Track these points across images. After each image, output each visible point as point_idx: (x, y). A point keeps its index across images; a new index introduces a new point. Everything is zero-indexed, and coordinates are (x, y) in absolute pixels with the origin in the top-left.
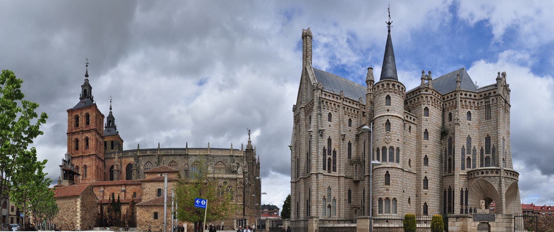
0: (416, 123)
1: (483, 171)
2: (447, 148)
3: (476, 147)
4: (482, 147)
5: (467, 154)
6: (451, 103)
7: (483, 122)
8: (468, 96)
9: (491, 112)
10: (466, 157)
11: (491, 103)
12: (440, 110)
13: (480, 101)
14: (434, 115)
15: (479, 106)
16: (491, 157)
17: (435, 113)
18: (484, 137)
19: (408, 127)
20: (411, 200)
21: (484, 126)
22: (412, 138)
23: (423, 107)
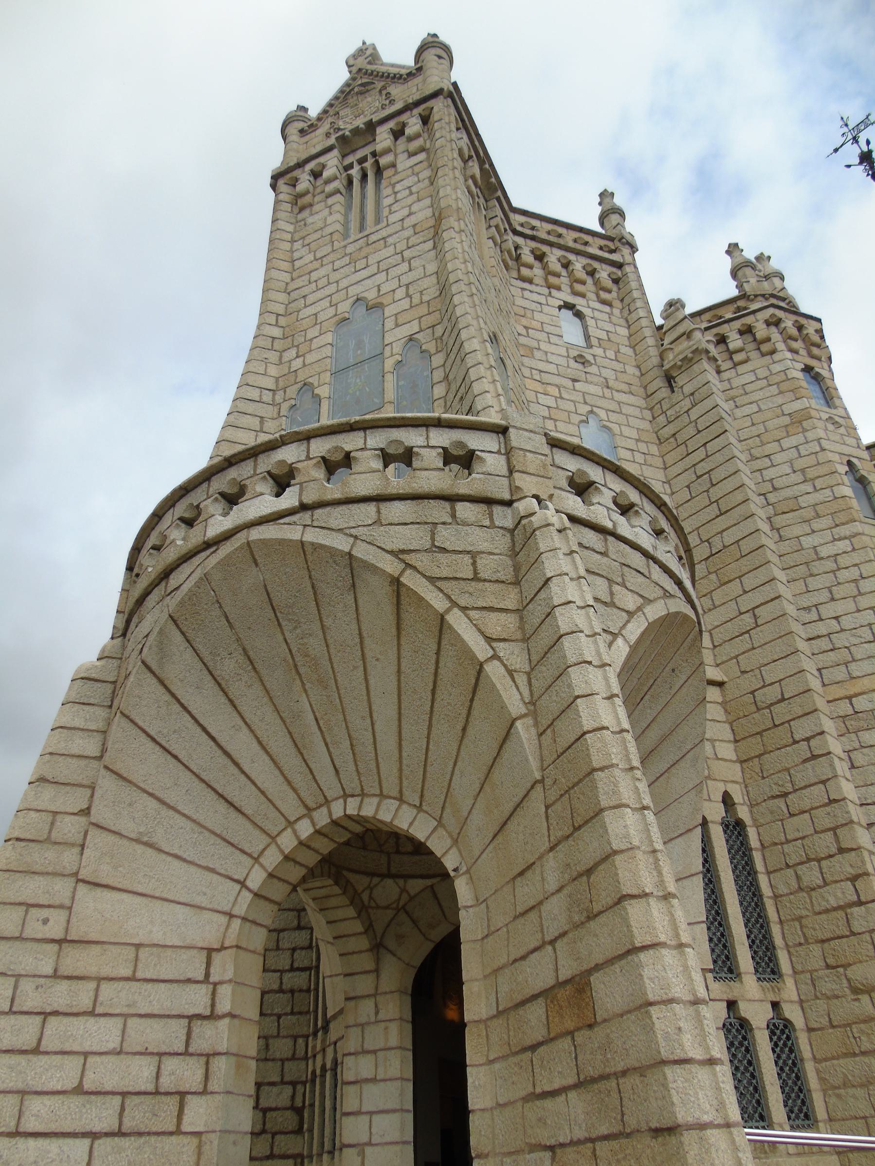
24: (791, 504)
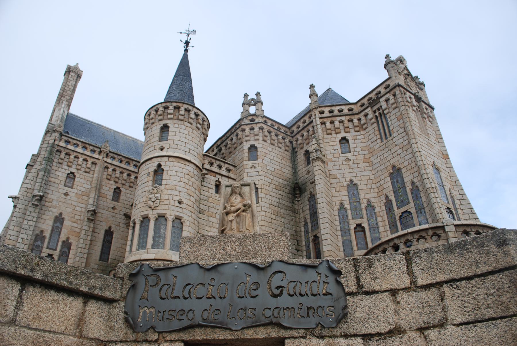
0: (232, 175)
1: (396, 241)
2: (308, 216)
3: (373, 200)
4: (387, 197)
5: (353, 219)
6: (305, 134)
7: (378, 146)
8: (336, 112)
9: (390, 124)
10: (352, 227)
11: (384, 107)
12: (286, 150)
13: (363, 113)
14: (272, 158)
15: (363, 122)
16: (413, 211)
17: (271, 153)
18: (387, 174)
19: (213, 183)
21: (383, 152)
23: (246, 146)
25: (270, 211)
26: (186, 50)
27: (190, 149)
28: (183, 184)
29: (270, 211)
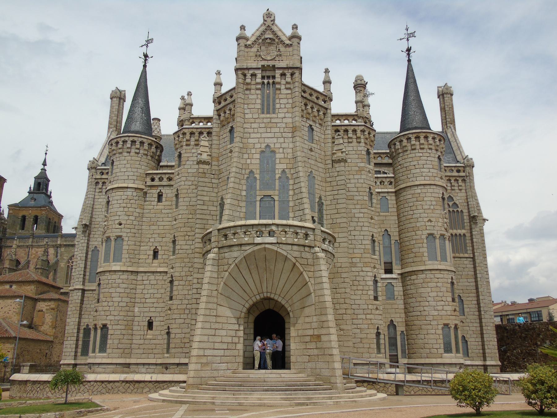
20: (154, 324)
22: (163, 211)
24: (352, 197)
25: (187, 212)
26: (145, 66)
27: (128, 176)
28: (122, 209)
29: (187, 212)
